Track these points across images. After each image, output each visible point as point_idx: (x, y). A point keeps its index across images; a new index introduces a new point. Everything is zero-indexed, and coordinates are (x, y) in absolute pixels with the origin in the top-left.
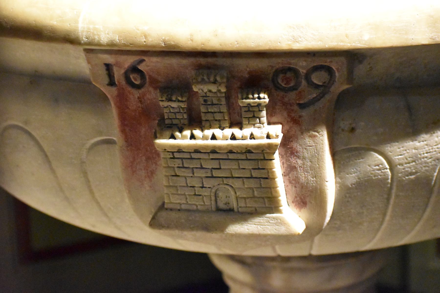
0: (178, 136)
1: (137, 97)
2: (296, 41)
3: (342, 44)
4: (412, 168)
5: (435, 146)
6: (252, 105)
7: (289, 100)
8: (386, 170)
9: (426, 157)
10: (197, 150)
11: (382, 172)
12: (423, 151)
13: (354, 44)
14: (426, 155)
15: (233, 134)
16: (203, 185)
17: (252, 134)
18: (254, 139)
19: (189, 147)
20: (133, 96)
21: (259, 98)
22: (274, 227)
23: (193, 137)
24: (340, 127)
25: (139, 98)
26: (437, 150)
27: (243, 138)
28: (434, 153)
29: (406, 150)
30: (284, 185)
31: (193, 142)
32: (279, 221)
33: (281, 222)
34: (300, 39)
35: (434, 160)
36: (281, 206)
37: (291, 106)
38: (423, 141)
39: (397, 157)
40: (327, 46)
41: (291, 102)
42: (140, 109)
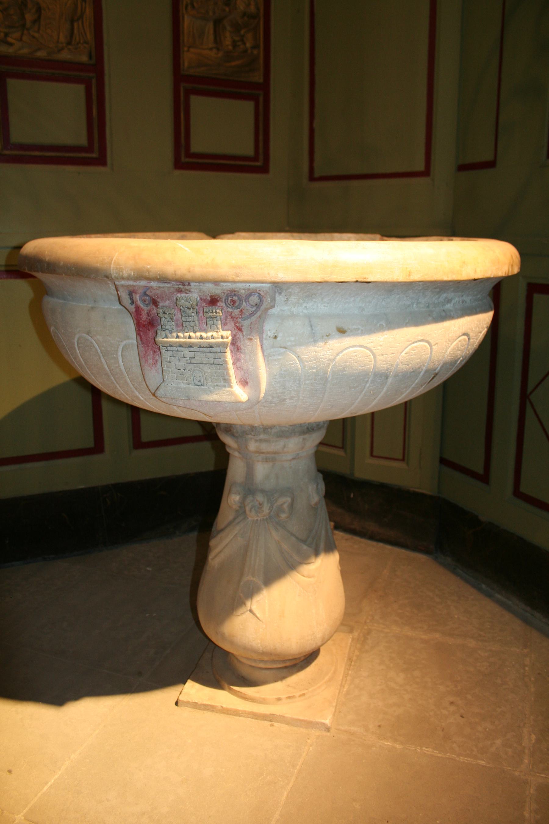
0: (169, 336)
1: (146, 312)
2: (237, 276)
3: (265, 279)
4: (314, 365)
5: (328, 351)
6: (212, 317)
7: (235, 315)
8: (297, 365)
9: (323, 358)
10: (181, 345)
11: (295, 366)
12: (320, 354)
13: (273, 279)
14: (322, 356)
15: (201, 336)
16: (185, 368)
17: (212, 336)
18: (214, 339)
19: (176, 342)
20: (144, 311)
21: (216, 312)
22: (228, 397)
23: (178, 337)
24: (268, 335)
25: (147, 313)
26: (329, 354)
27: (207, 338)
28: (328, 355)
29: (309, 353)
30: (243, 392)
31: (177, 340)
32: (231, 393)
33: (232, 394)
34: (240, 275)
35: (328, 360)
36: (232, 383)
37: (236, 319)
38: (320, 347)
39: (304, 357)
40: (256, 280)
41: (236, 316)
42: (148, 320)
